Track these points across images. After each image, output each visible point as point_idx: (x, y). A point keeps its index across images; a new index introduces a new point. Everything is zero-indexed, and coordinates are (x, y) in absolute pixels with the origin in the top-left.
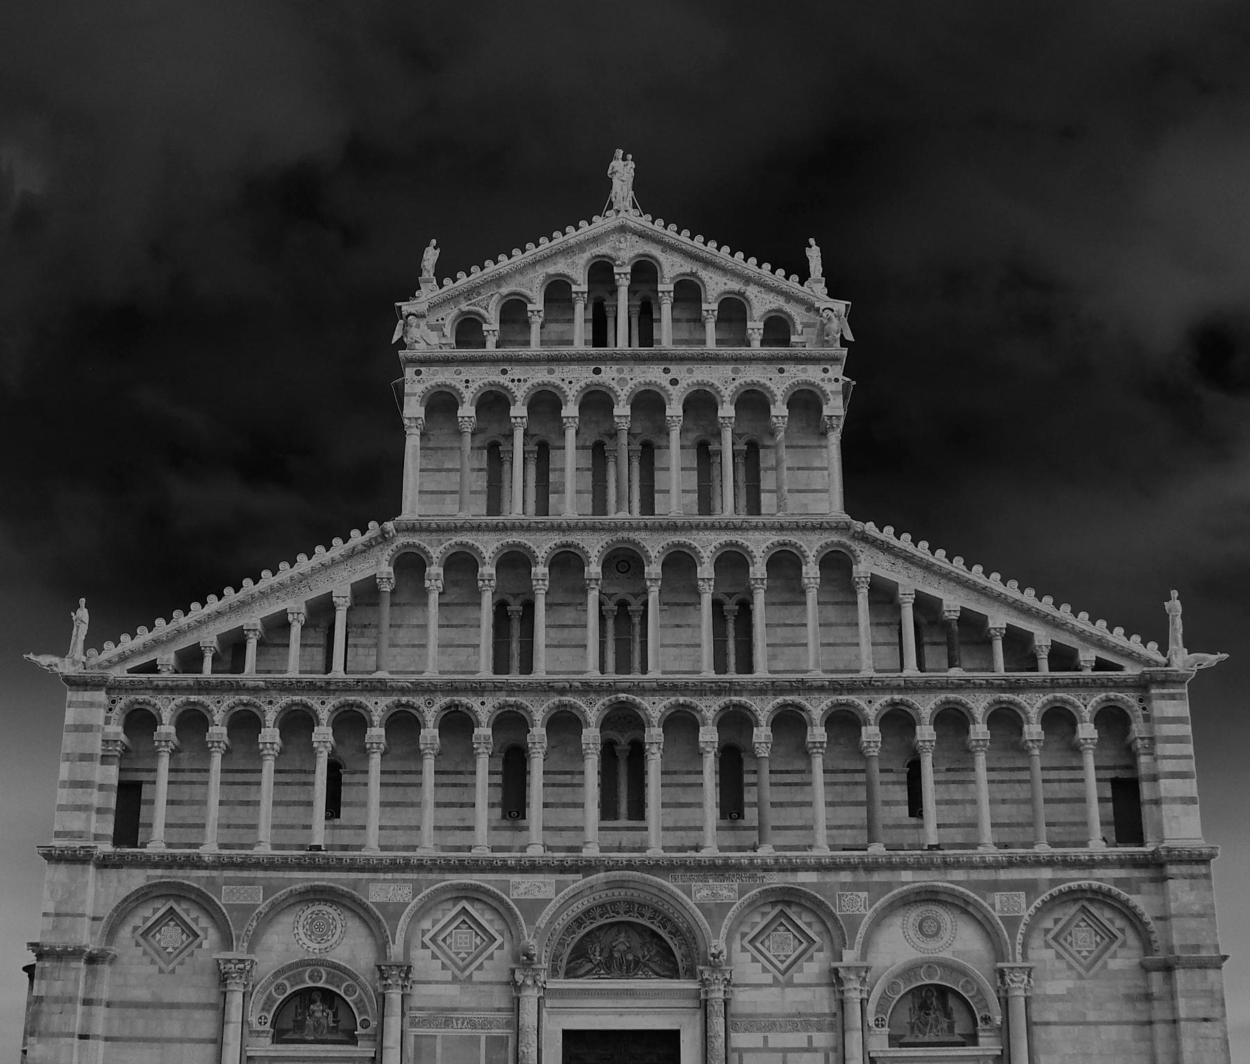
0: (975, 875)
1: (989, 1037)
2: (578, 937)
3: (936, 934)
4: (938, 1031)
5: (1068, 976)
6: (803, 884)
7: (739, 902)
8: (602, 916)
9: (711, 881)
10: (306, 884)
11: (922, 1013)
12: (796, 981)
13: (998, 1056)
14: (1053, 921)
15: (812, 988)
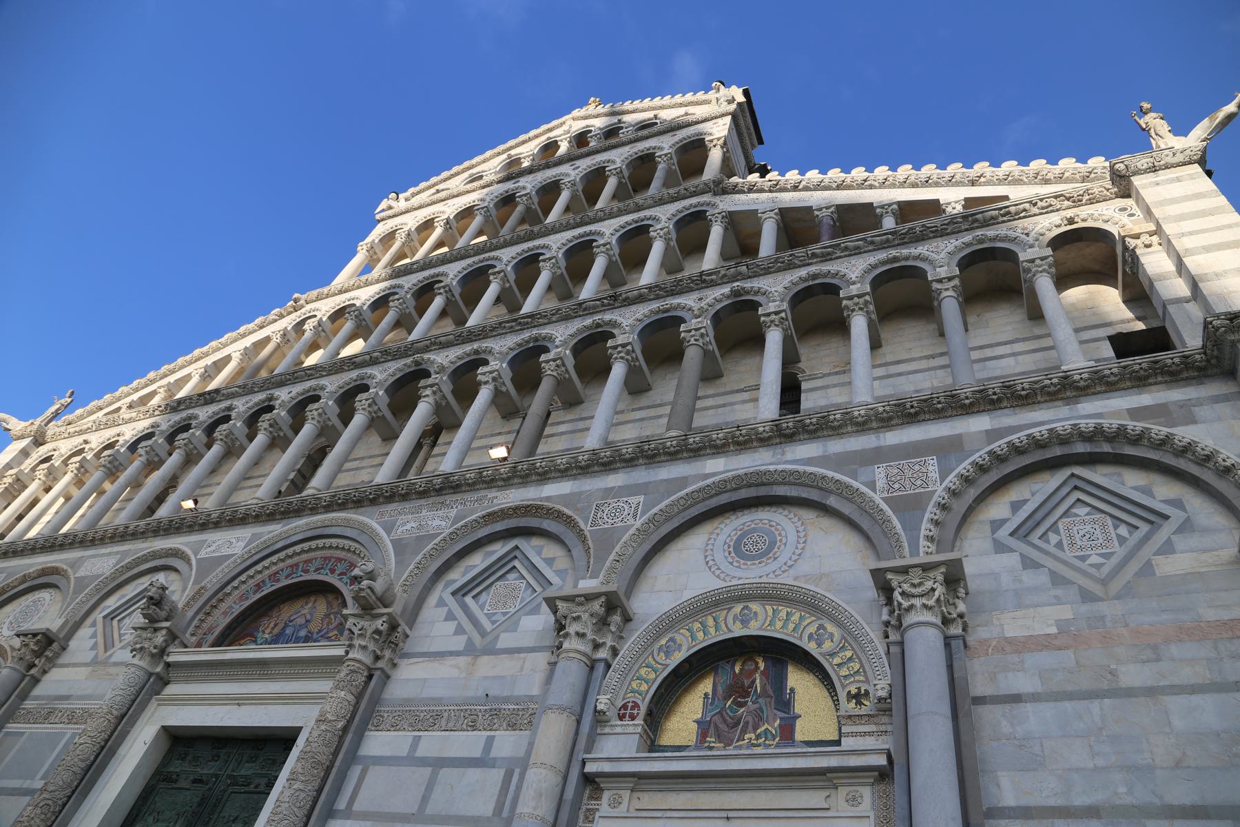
0: (836, 446)
1: (865, 734)
2: (247, 603)
3: (767, 552)
4: (758, 737)
5: (1055, 597)
6: (548, 499)
7: (447, 531)
8: (287, 577)
9: (424, 511)
10: (40, 567)
11: (729, 703)
12: (501, 644)
13: (883, 775)
14: (1008, 506)
15: (522, 655)
